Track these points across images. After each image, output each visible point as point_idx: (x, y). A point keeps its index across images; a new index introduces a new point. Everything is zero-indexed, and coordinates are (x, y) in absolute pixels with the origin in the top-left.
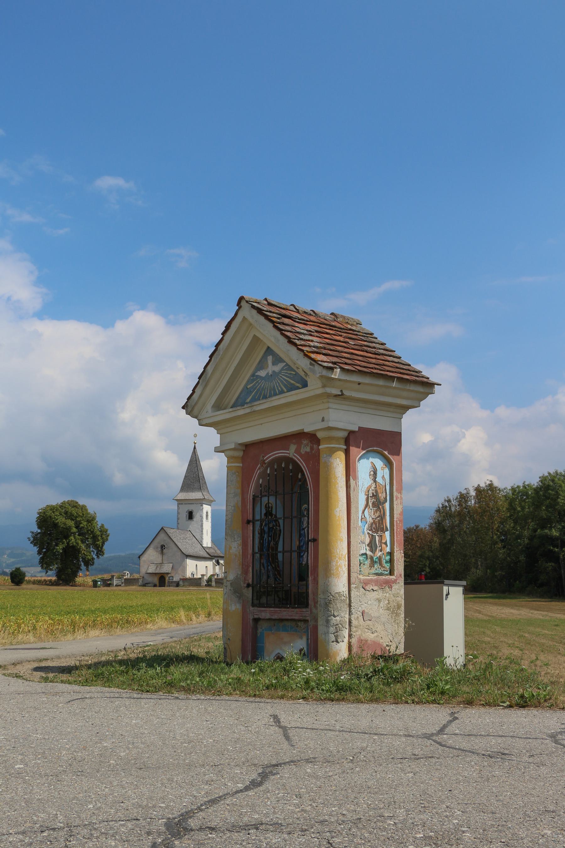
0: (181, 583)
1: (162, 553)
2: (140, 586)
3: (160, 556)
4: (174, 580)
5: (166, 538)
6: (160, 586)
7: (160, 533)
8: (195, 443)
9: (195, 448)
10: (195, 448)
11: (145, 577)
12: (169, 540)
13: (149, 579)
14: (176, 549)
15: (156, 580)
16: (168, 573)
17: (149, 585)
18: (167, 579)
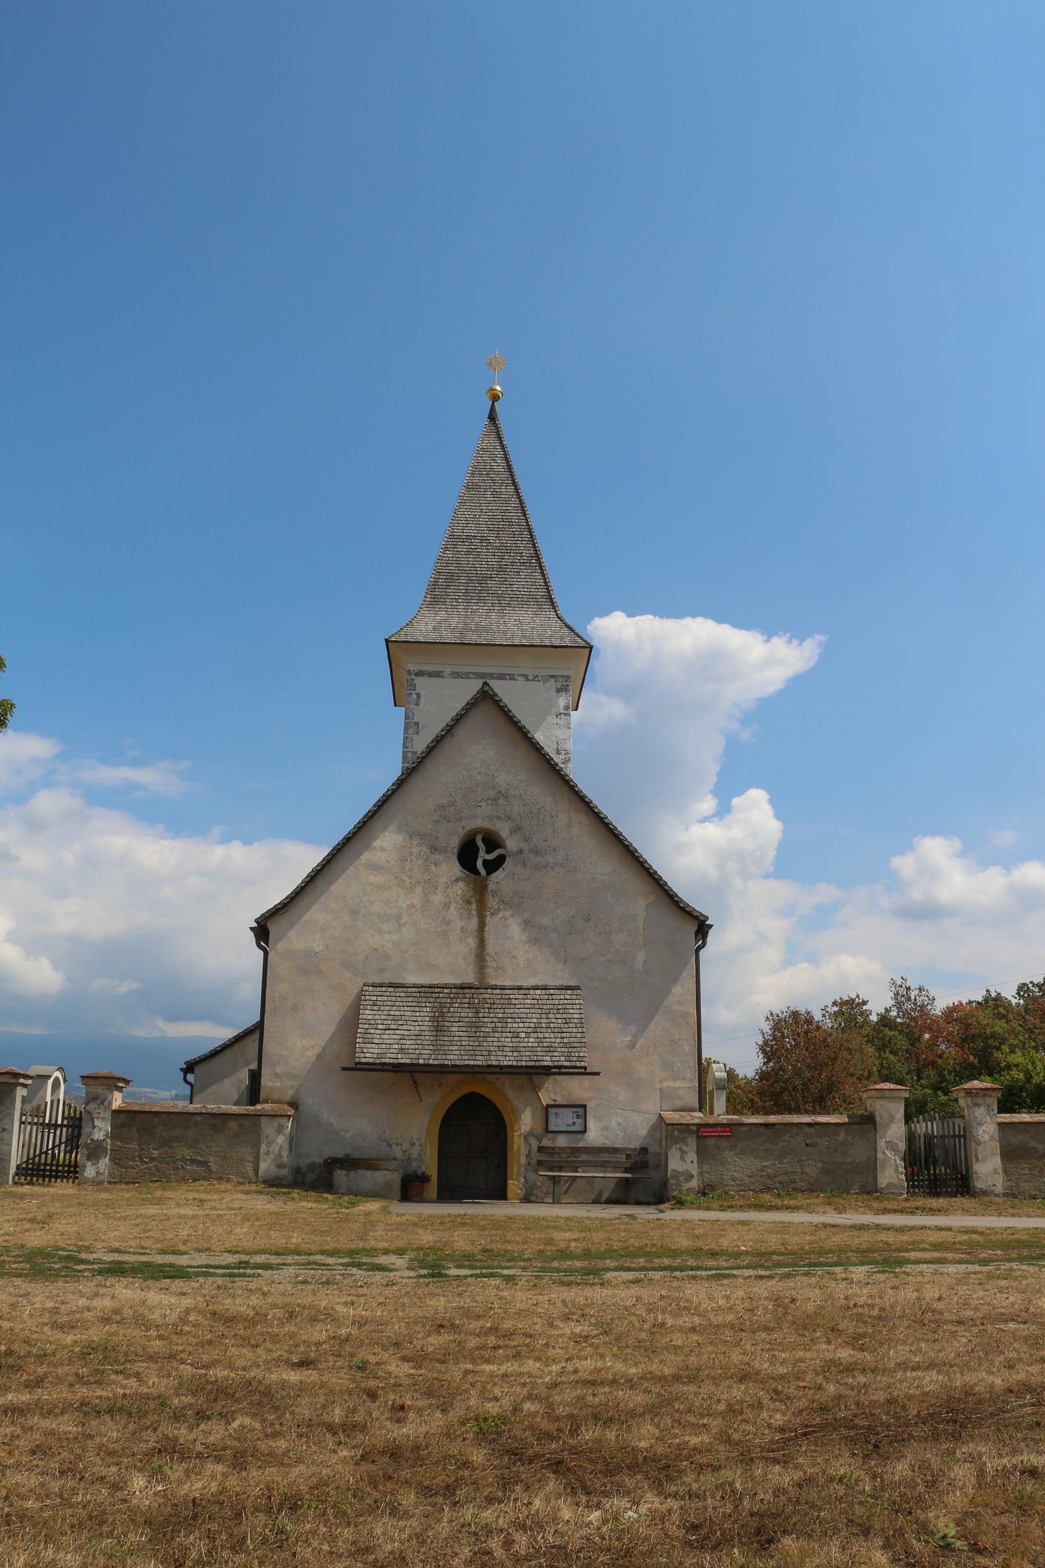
0: (682, 1162)
1: (479, 897)
2: (273, 1183)
3: (460, 921)
4: (595, 1135)
5: (516, 778)
6: (449, 1193)
7: (463, 732)
8: (495, 398)
9: (492, 417)
10: (492, 417)
11: (311, 1103)
12: (536, 793)
13: (356, 1123)
14: (604, 866)
15: (414, 1132)
16: (534, 1074)
17: (368, 1178)
18: (526, 1121)
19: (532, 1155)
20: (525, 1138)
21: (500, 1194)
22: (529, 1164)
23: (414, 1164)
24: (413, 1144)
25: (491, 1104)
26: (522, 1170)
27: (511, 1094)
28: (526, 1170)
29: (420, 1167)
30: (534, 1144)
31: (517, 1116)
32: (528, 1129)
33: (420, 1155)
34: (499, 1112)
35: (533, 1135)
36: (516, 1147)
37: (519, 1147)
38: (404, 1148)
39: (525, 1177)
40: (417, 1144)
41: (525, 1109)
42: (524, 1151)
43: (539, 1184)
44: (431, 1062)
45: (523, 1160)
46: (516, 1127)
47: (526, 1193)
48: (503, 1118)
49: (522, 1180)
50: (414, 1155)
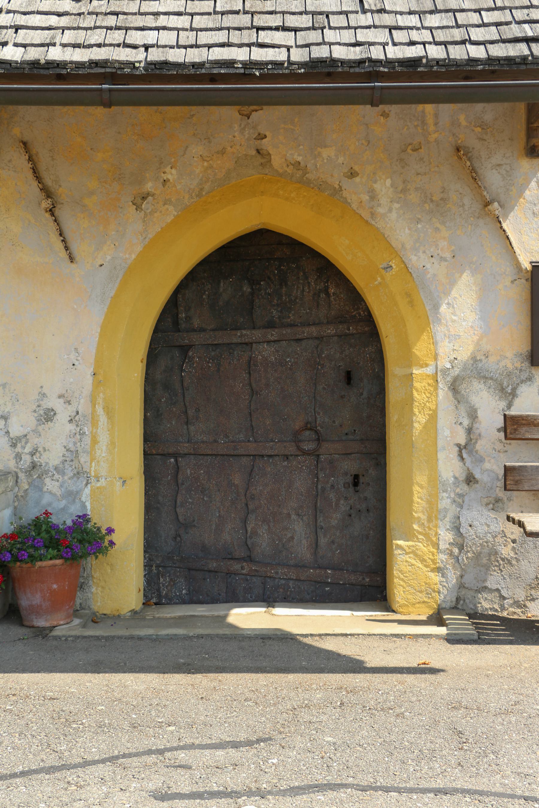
19: (481, 446)
20: (454, 388)
21: (370, 588)
22: (470, 480)
23: (51, 484)
24: (49, 416)
25: (326, 269)
26: (445, 502)
27: (398, 225)
28: (460, 502)
29: (73, 496)
30: (490, 412)
31: (422, 310)
32: (464, 354)
33: (72, 454)
34: (355, 297)
35: (484, 377)
36: (420, 419)
37: (433, 418)
38: (16, 430)
39: (457, 528)
40: (63, 413)
41: (453, 283)
42: (450, 432)
43: (506, 551)
44: (55, 54)
45: (449, 467)
46: (420, 349)
47: (461, 586)
48: (369, 319)
49: (446, 537)
50: (52, 457)
